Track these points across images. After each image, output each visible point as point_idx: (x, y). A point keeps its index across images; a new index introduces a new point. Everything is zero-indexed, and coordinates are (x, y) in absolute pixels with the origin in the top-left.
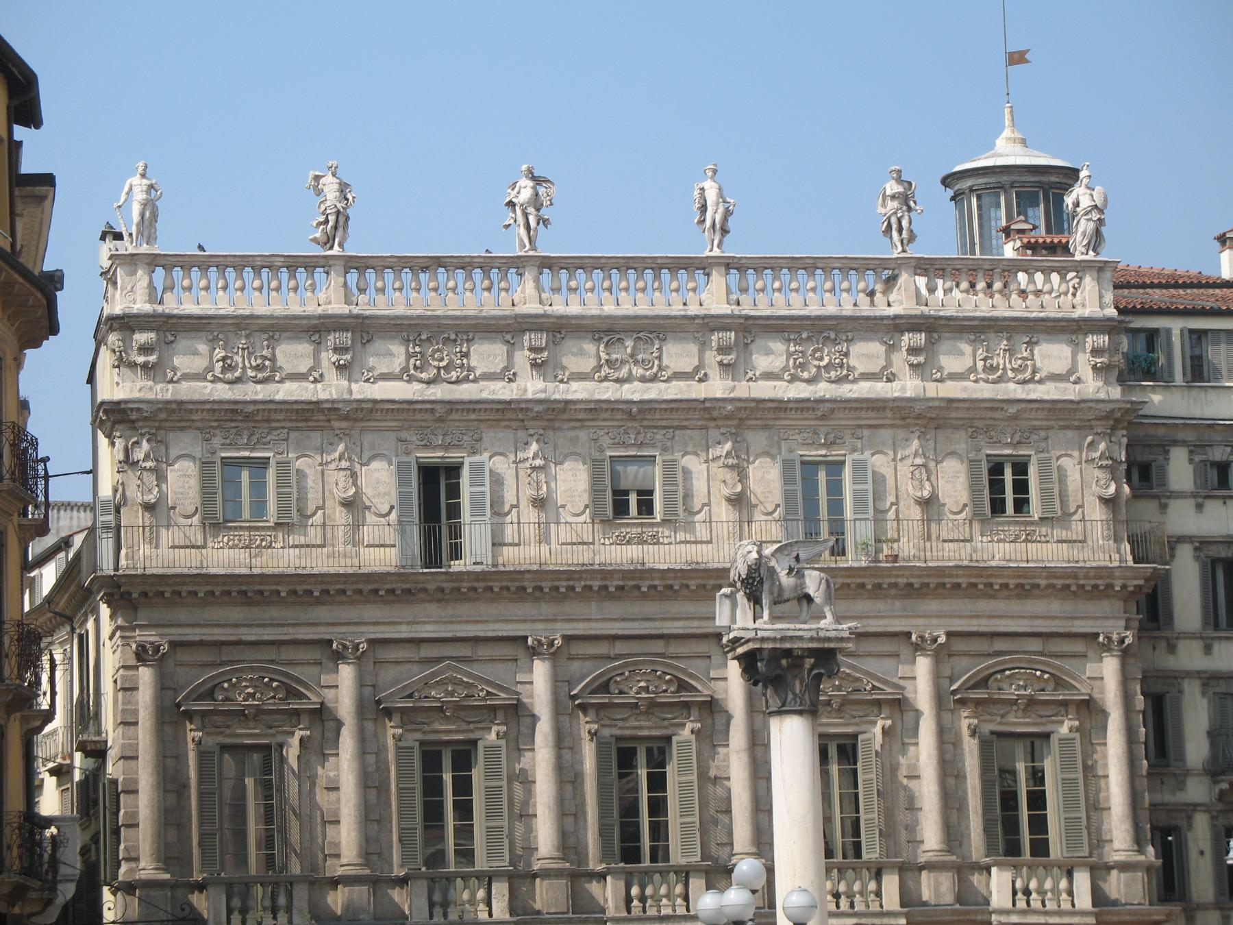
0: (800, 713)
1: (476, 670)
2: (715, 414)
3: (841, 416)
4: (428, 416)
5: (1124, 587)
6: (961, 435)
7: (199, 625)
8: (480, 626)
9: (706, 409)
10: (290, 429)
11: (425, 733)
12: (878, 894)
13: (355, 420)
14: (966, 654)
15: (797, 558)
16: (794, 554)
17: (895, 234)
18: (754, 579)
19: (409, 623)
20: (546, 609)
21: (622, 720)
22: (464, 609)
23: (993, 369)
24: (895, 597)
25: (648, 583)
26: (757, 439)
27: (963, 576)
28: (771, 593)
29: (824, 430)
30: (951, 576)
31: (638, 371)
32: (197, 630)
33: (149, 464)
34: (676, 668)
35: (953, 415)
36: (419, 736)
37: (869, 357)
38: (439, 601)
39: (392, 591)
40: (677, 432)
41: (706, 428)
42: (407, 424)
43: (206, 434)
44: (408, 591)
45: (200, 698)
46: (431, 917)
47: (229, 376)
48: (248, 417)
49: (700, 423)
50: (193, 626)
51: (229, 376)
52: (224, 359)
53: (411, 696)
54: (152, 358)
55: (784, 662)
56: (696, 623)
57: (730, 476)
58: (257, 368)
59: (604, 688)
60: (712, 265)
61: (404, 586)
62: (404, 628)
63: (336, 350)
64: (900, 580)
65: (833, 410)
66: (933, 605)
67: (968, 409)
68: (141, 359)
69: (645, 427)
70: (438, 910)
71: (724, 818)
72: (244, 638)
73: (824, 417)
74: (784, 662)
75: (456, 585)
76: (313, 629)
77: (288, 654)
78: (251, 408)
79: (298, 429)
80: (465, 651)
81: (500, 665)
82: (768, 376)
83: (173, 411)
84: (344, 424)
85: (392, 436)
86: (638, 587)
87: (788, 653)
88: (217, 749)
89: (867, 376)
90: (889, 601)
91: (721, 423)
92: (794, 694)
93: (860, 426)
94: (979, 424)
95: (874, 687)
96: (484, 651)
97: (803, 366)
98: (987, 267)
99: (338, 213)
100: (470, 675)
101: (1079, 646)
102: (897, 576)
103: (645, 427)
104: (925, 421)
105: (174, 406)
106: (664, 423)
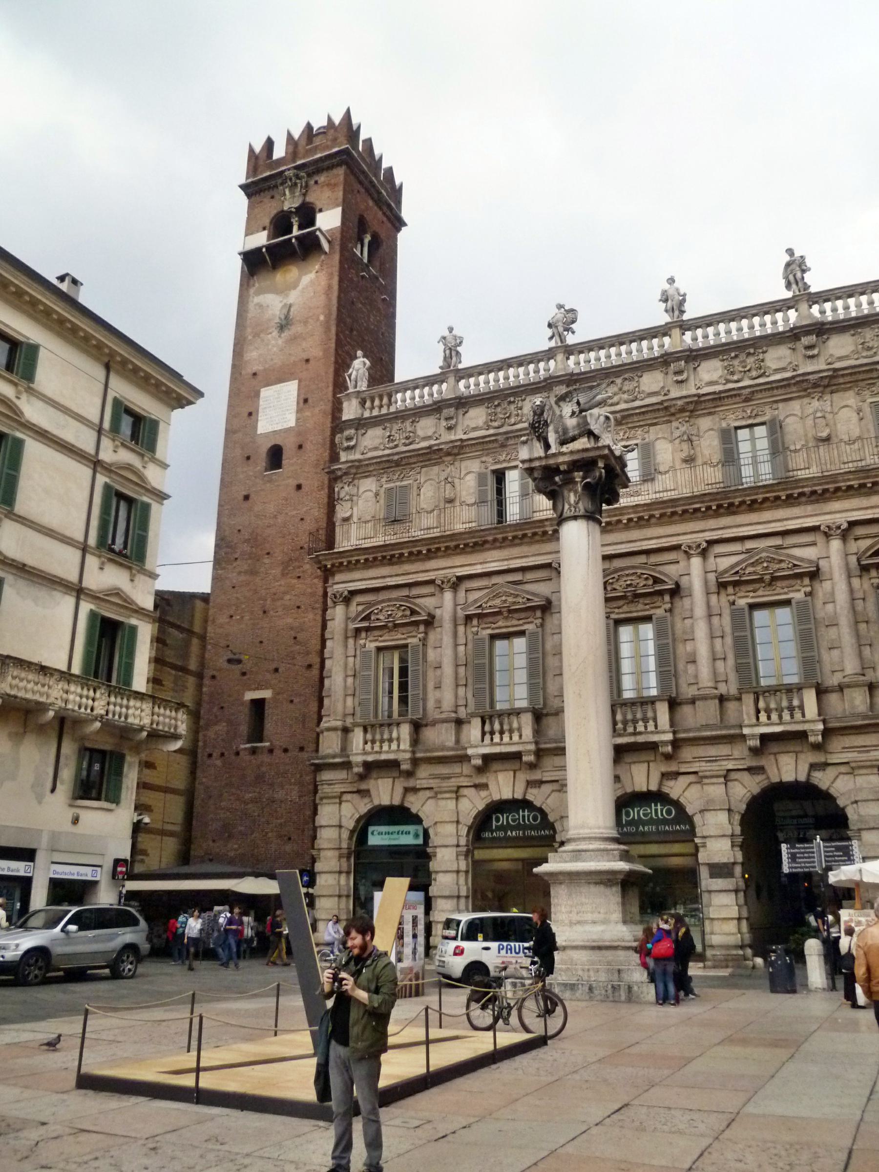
0: (575, 518)
1: (528, 587)
2: (673, 410)
3: (760, 396)
4: (495, 445)
6: (851, 393)
7: (365, 580)
8: (524, 560)
9: (666, 408)
10: (422, 467)
11: (493, 629)
12: (801, 707)
13: (456, 455)
14: (867, 537)
15: (578, 403)
16: (575, 400)
17: (794, 286)
18: (539, 422)
19: (481, 563)
21: (619, 608)
23: (869, 349)
24: (806, 503)
25: (626, 517)
26: (705, 423)
27: (854, 479)
28: (556, 432)
29: (751, 408)
30: (844, 481)
31: (625, 396)
32: (364, 582)
33: (347, 497)
34: (660, 572)
35: (841, 380)
36: (490, 631)
37: (779, 359)
38: (500, 548)
39: (466, 545)
40: (651, 428)
41: (671, 422)
42: (486, 452)
43: (379, 477)
44: (476, 544)
45: (361, 620)
46: (483, 740)
47: (391, 445)
48: (398, 464)
49: (665, 419)
50: (361, 580)
51: (391, 445)
52: (389, 437)
53: (480, 606)
54: (352, 443)
55: (557, 479)
56: (664, 540)
57: (685, 446)
58: (407, 438)
60: (670, 329)
61: (474, 540)
62: (479, 566)
63: (447, 419)
64: (806, 490)
65: (753, 392)
66: (836, 505)
67: (851, 374)
68: (346, 445)
69: (629, 428)
71: (691, 668)
72: (389, 584)
73: (747, 400)
74: (557, 479)
75: (504, 535)
76: (427, 574)
77: (415, 591)
78: (396, 458)
79: (426, 466)
80: (517, 577)
81: (542, 584)
82: (711, 383)
83: (358, 467)
84: (449, 458)
85: (478, 460)
86: (619, 521)
88: (373, 650)
89: (777, 371)
90: (803, 507)
91: (678, 416)
92: (570, 505)
93: (776, 402)
95: (795, 565)
96: (530, 576)
97: (732, 373)
98: (860, 290)
99: (450, 349)
100: (516, 590)
102: (803, 487)
103: (629, 428)
104: (821, 389)
105: (357, 464)
106: (641, 423)
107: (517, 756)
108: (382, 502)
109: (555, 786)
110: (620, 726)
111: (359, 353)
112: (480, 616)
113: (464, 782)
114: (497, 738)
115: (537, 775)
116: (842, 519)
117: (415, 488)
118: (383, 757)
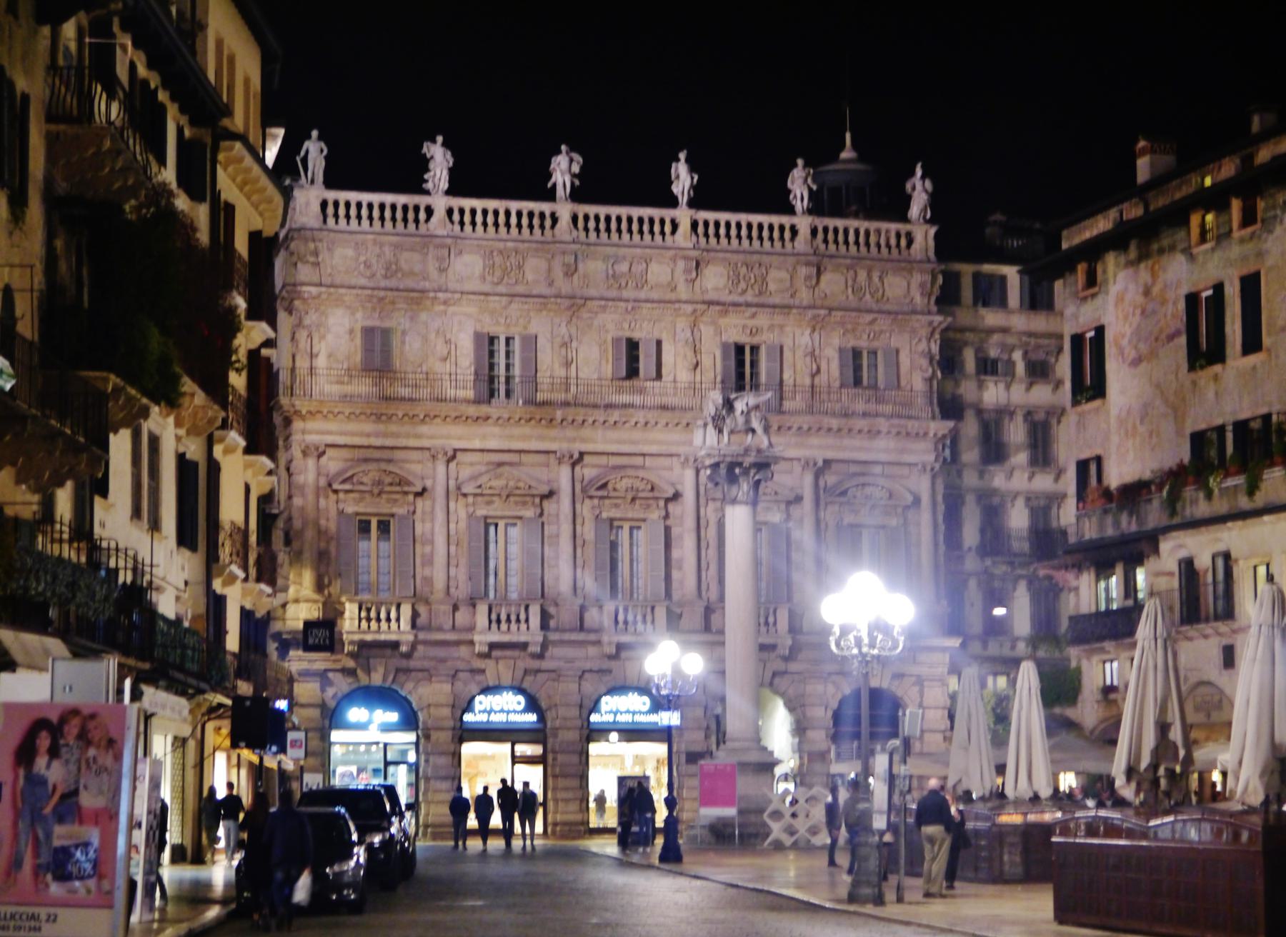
0: (747, 503)
5: (935, 435)
20: (570, 433)
22: (517, 431)
37: (781, 281)
45: (344, 482)
53: (480, 487)
59: (604, 486)
66: (814, 441)
70: (494, 625)
87: (740, 464)
94: (849, 327)
96: (525, 458)
101: (905, 471)
107: (523, 646)
108: (358, 341)
109: (553, 675)
110: (621, 625)
111: (315, 133)
112: (475, 495)
113: (461, 665)
114: (504, 626)
115: (535, 664)
116: (820, 457)
117: (399, 334)
118: (383, 637)
